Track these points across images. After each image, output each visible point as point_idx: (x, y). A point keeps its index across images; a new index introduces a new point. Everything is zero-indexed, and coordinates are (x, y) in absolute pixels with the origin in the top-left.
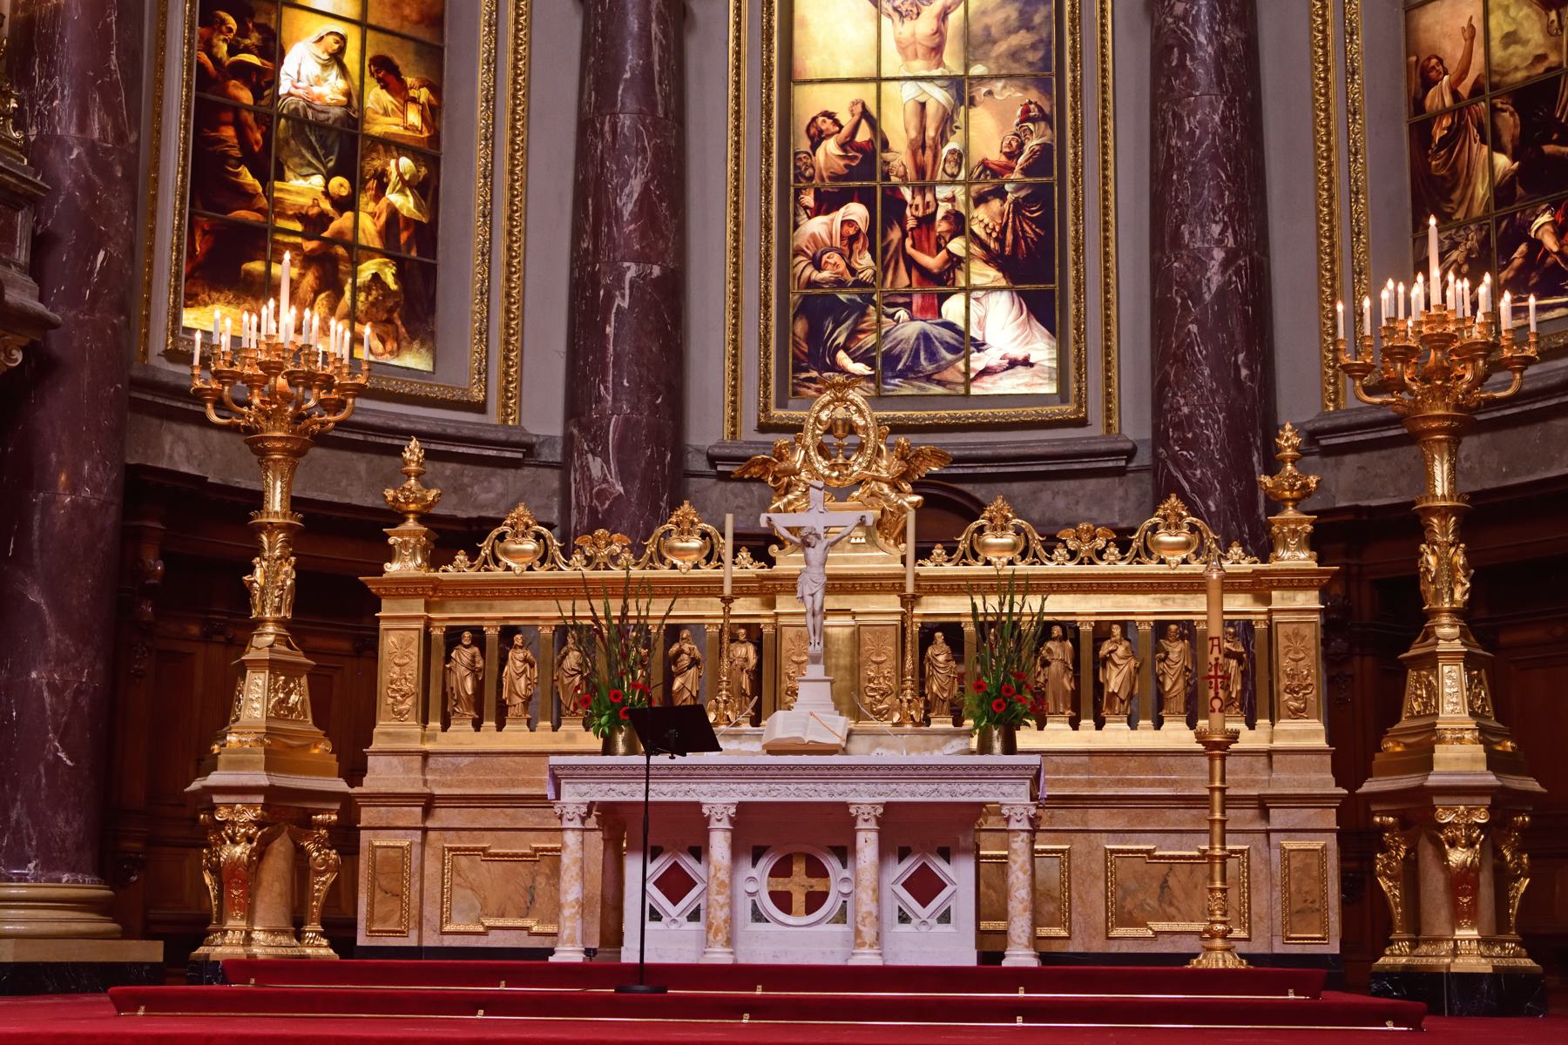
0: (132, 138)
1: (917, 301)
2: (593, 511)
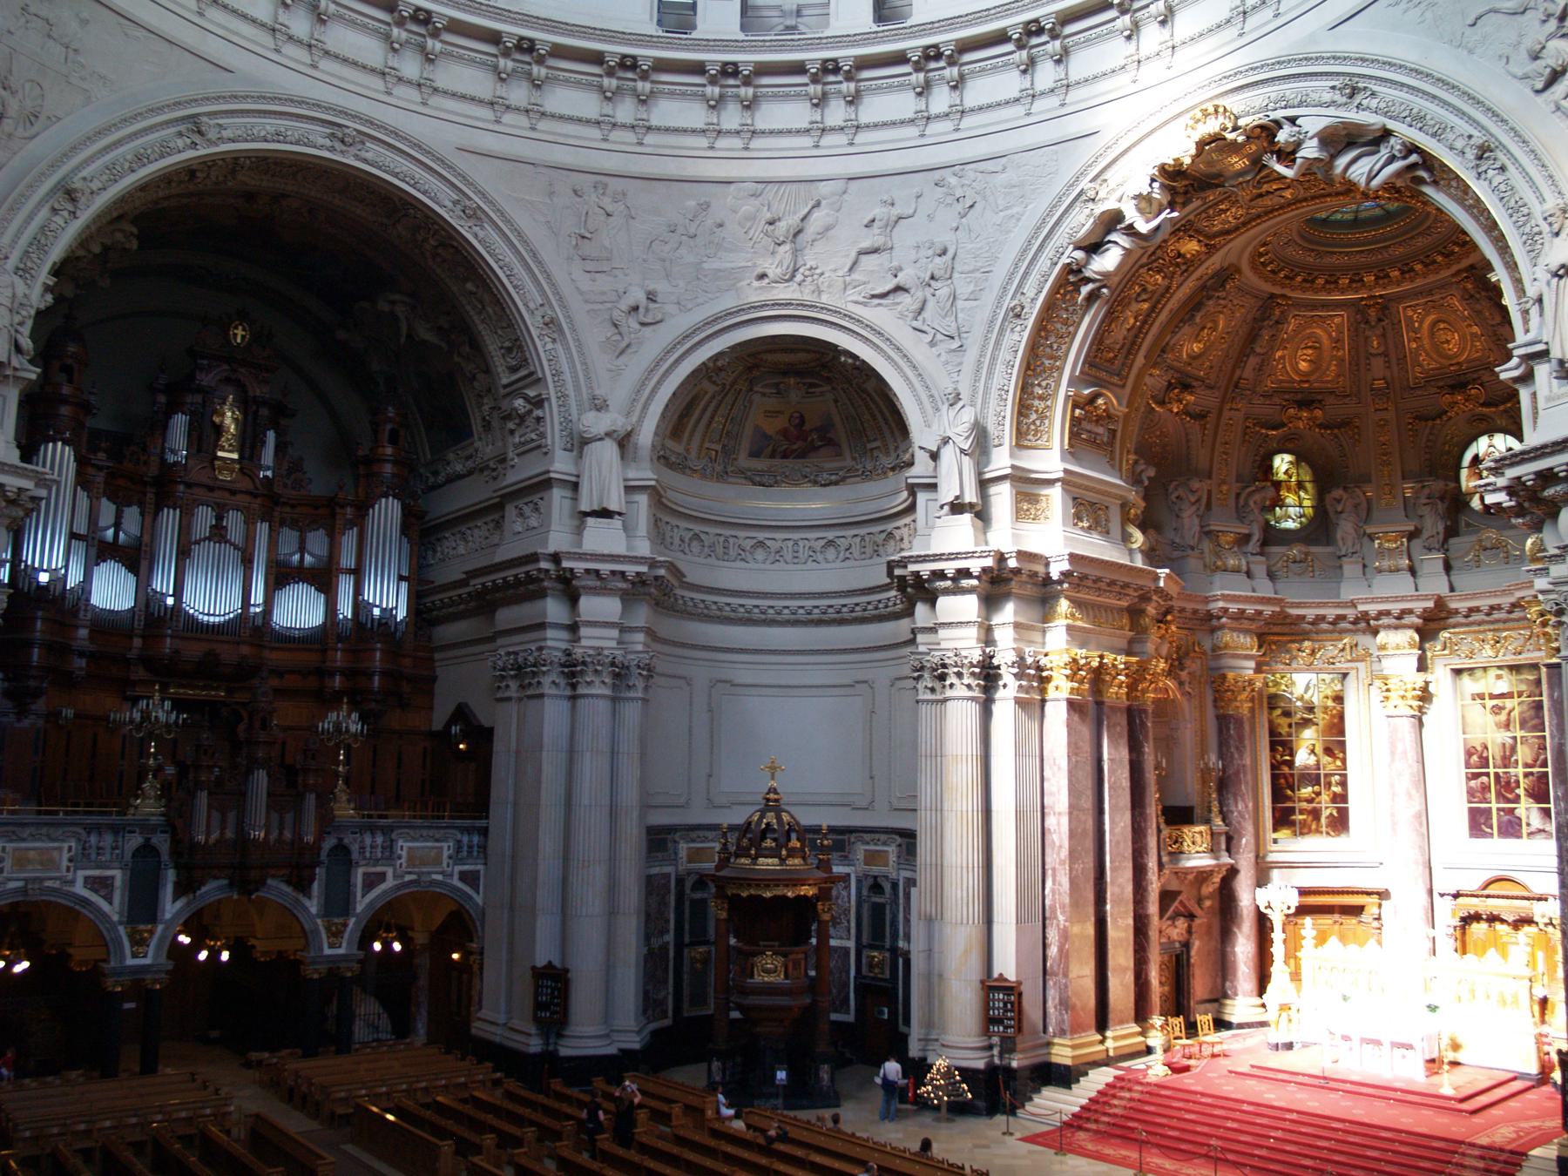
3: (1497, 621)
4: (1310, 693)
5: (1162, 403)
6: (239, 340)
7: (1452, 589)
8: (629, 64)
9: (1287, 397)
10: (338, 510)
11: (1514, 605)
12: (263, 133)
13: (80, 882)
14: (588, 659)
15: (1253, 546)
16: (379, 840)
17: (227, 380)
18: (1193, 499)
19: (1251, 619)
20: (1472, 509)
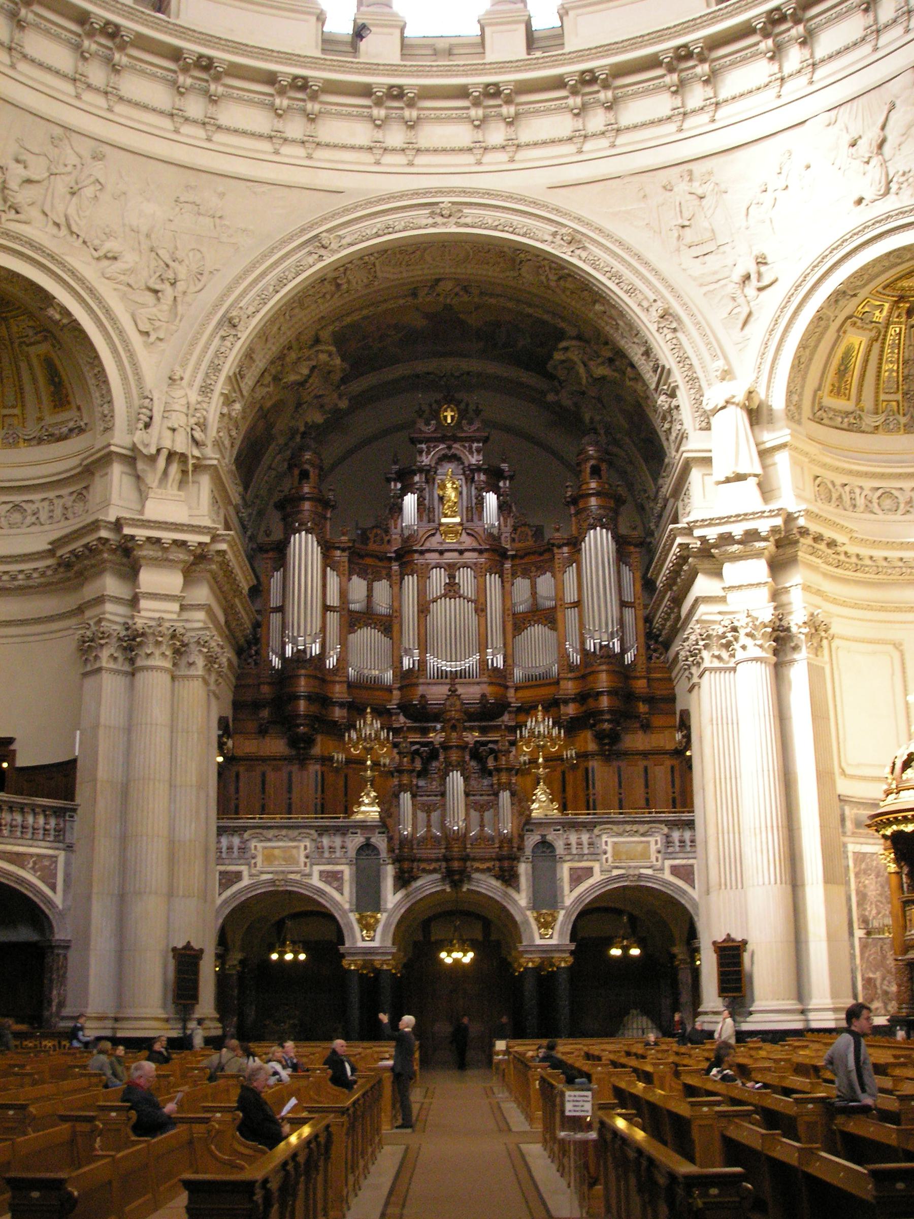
6: (449, 421)
8: (683, 54)
10: (556, 550)
12: (375, 231)
13: (316, 875)
14: (736, 624)
16: (585, 837)
17: (445, 458)
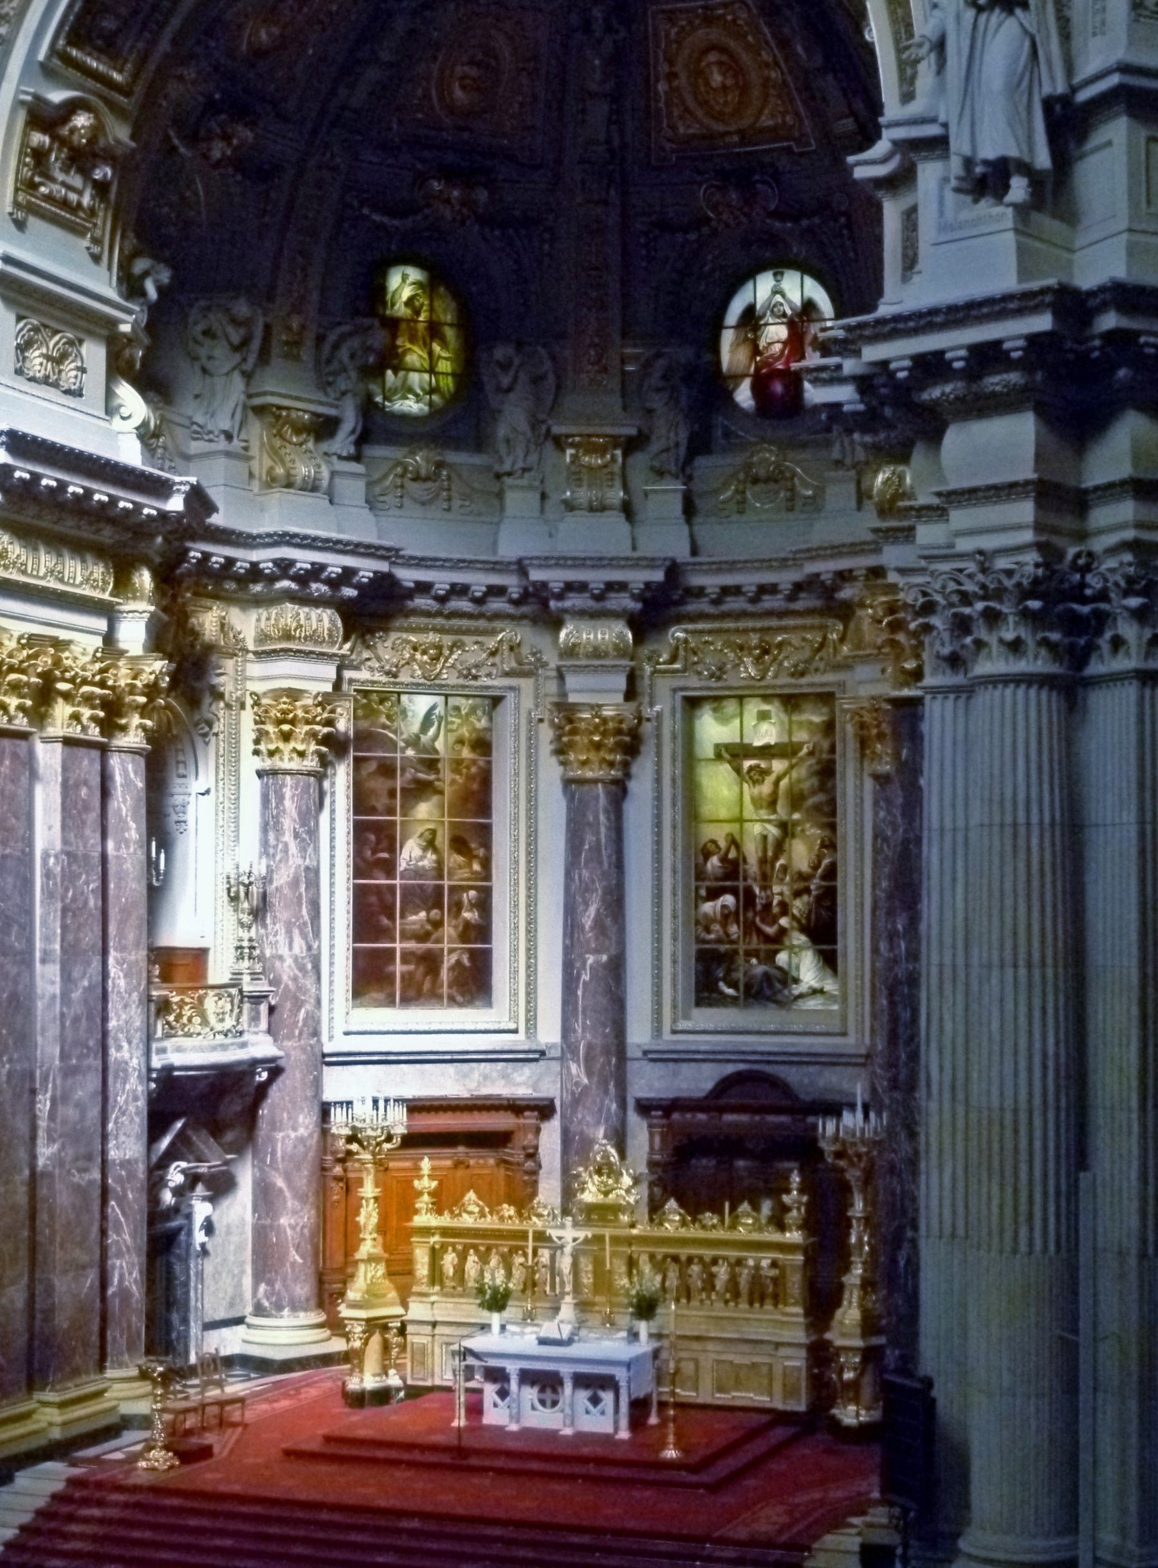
0: (315, 946)
1: (762, 955)
2: (573, 1093)
3: (769, 614)
4: (432, 732)
5: (193, 139)
7: (694, 552)
9: (426, 154)
11: (798, 587)
15: (342, 442)
18: (236, 338)
19: (335, 583)
20: (736, 406)
